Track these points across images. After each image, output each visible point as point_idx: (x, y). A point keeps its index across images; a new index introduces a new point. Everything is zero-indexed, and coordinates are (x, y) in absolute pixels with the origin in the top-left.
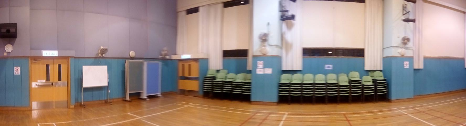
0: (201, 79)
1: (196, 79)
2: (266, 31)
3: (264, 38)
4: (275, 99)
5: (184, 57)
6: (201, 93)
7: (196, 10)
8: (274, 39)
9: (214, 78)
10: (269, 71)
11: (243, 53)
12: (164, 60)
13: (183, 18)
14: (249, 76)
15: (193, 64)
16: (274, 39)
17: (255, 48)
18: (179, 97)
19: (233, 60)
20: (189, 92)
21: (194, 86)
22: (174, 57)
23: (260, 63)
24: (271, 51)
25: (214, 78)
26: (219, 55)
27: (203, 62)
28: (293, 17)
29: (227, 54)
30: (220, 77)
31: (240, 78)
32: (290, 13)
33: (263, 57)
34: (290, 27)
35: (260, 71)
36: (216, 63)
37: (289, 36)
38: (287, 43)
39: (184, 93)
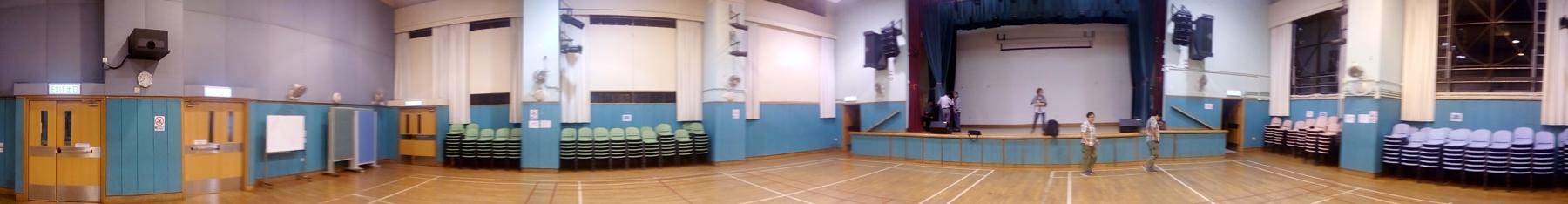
0: (440, 139)
1: (431, 138)
2: (541, 68)
3: (540, 79)
4: (556, 165)
5: (409, 104)
6: (440, 159)
7: (427, 32)
8: (552, 80)
9: (462, 136)
10: (547, 124)
11: (503, 99)
12: (377, 107)
13: (405, 46)
14: (515, 131)
15: (426, 115)
16: (552, 80)
17: (527, 90)
18: (401, 166)
19: (486, 109)
20: (418, 158)
21: (427, 149)
22: (390, 104)
23: (534, 113)
24: (549, 96)
25: (462, 136)
26: (466, 101)
27: (440, 112)
28: (579, 49)
29: (477, 100)
30: (471, 134)
31: (502, 135)
32: (574, 44)
33: (539, 104)
34: (572, 62)
35: (533, 125)
36: (460, 115)
37: (572, 74)
38: (568, 84)
39: (408, 159)
